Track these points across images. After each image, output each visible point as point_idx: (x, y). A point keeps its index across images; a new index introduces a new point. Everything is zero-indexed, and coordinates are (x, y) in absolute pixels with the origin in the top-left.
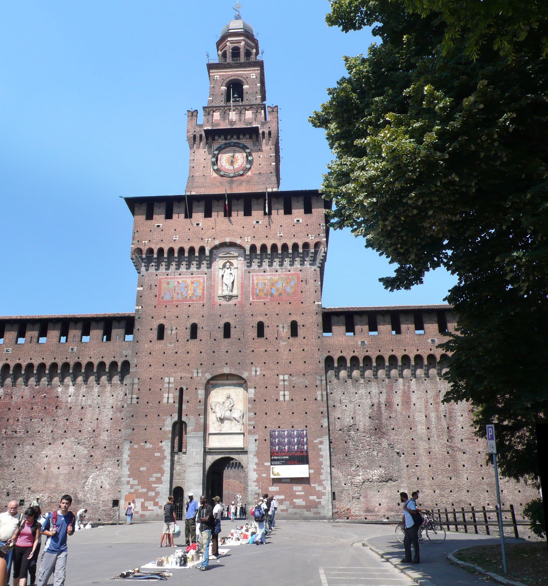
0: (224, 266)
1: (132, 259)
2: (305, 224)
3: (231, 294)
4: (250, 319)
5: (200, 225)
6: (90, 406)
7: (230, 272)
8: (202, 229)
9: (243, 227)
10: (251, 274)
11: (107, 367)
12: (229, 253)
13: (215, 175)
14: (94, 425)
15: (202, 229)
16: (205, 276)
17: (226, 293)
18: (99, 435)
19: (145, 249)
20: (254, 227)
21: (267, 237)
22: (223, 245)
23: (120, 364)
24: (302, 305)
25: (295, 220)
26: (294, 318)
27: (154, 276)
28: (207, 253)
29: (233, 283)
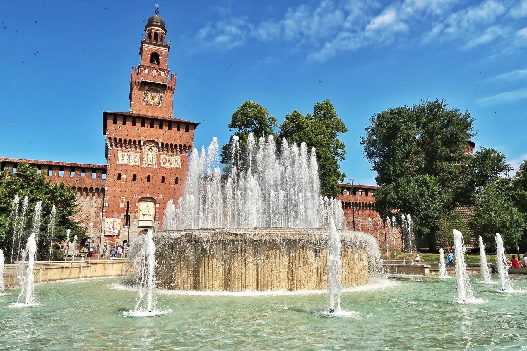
3: (151, 163)
4: (158, 174)
5: (139, 130)
6: (85, 206)
11: (94, 190)
13: (144, 103)
14: (87, 214)
17: (149, 163)
18: (90, 219)
19: (112, 138)
22: (149, 141)
23: (100, 189)
24: (181, 171)
26: (177, 176)
27: (116, 151)
28: (142, 144)
29: (152, 158)
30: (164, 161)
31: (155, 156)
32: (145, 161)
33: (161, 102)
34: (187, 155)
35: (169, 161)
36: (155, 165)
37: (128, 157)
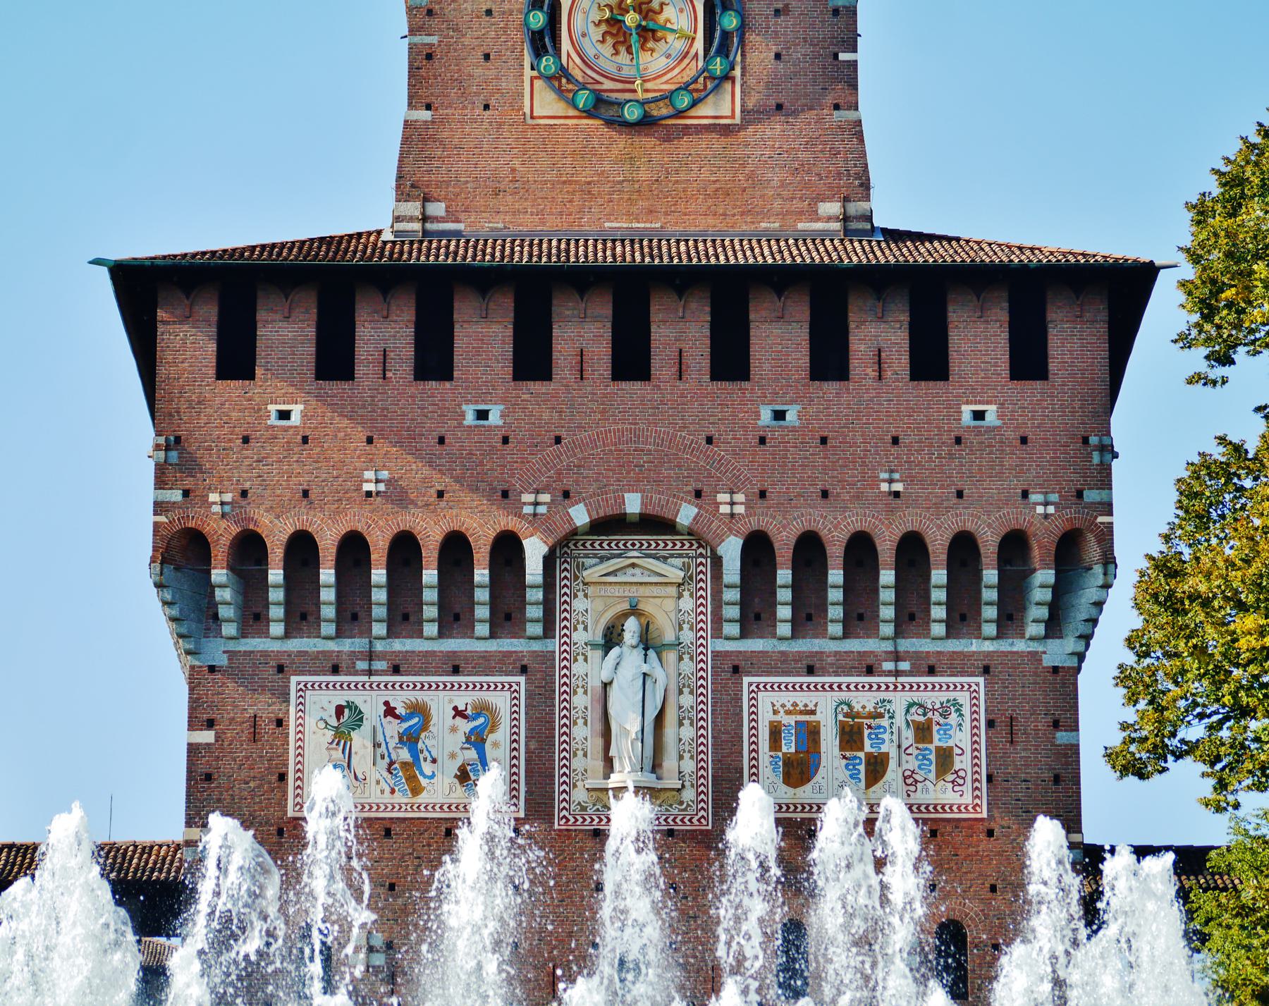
0: (611, 638)
1: (159, 586)
2: (1012, 435)
5: (494, 418)
7: (645, 668)
8: (505, 440)
9: (709, 440)
10: (746, 680)
12: (633, 565)
15: (505, 440)
16: (522, 679)
19: (222, 534)
20: (762, 441)
21: (825, 494)
25: (967, 410)
29: (660, 719)
30: (789, 747)
31: (687, 700)
32: (578, 763)
33: (718, 66)
34: (1057, 652)
35: (850, 737)
36: (689, 795)
37: (393, 728)
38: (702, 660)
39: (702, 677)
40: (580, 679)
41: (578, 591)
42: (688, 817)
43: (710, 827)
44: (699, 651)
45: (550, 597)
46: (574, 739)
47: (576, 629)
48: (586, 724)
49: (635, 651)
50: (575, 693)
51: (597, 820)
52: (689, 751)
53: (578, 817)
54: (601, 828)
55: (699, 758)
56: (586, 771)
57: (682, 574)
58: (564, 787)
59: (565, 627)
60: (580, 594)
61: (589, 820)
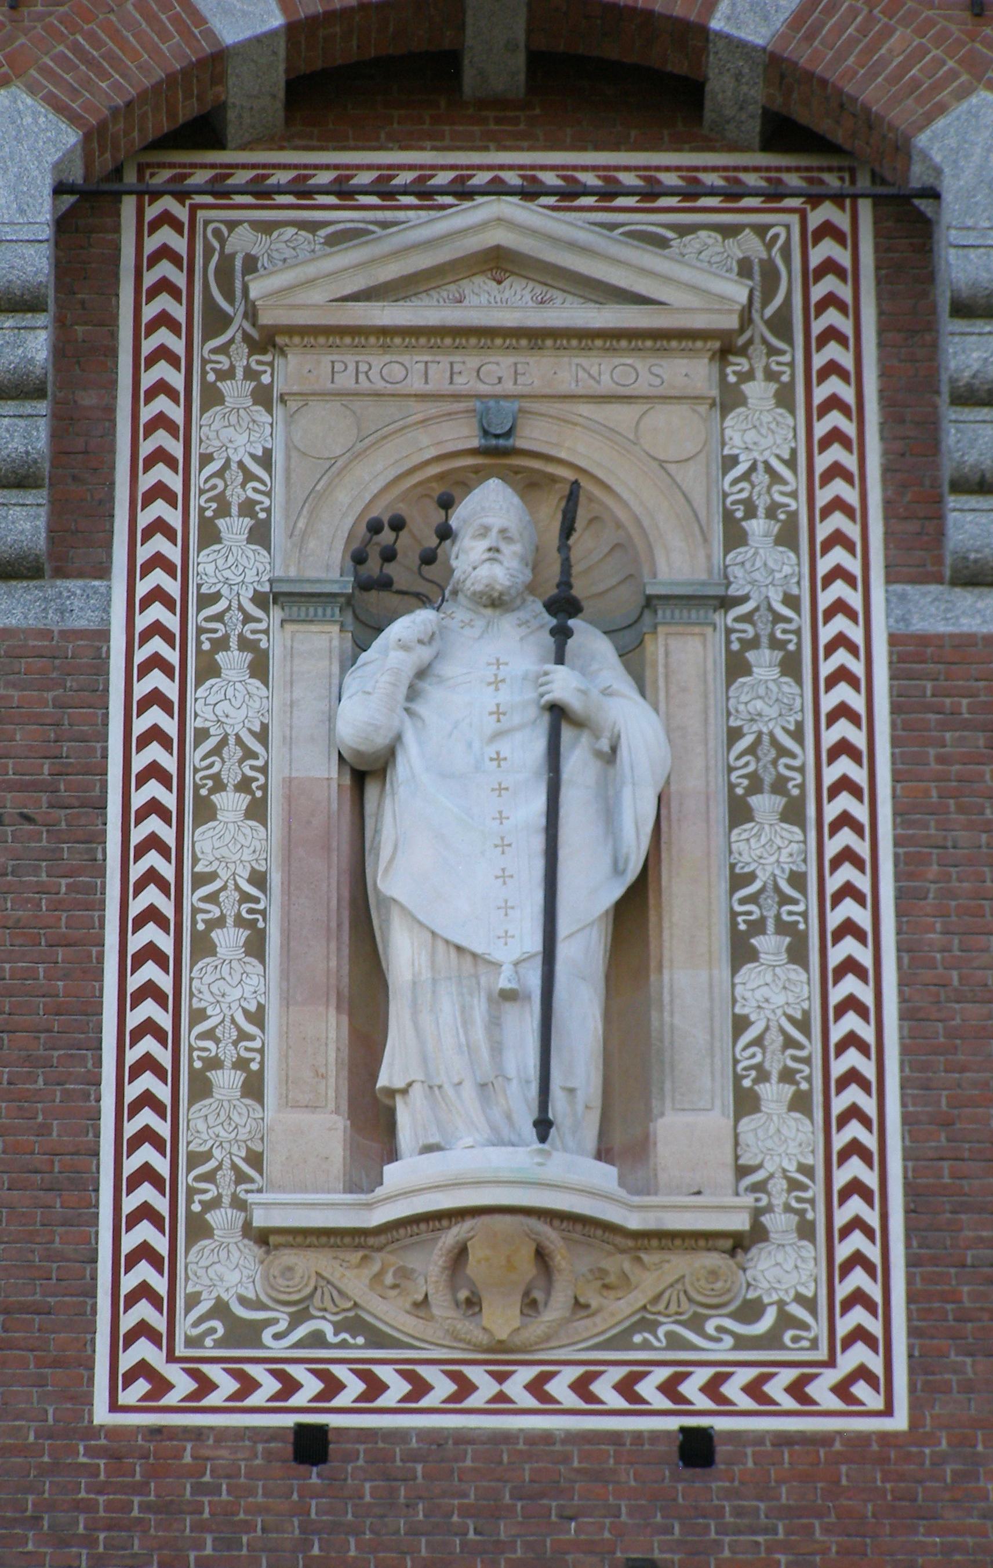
38: (842, 675)
39: (843, 748)
40: (233, 752)
41: (229, 374)
42: (788, 1376)
43: (899, 1422)
44: (826, 634)
45: (88, 399)
46: (197, 1016)
47: (210, 536)
48: (256, 947)
49: (507, 625)
50: (206, 812)
51: (312, 1386)
52: (787, 1076)
53: (214, 1372)
54: (334, 1421)
55: (839, 1104)
56: (255, 1160)
57: (739, 292)
58: (145, 1232)
59: (159, 526)
60: (236, 391)
61: (270, 1386)
